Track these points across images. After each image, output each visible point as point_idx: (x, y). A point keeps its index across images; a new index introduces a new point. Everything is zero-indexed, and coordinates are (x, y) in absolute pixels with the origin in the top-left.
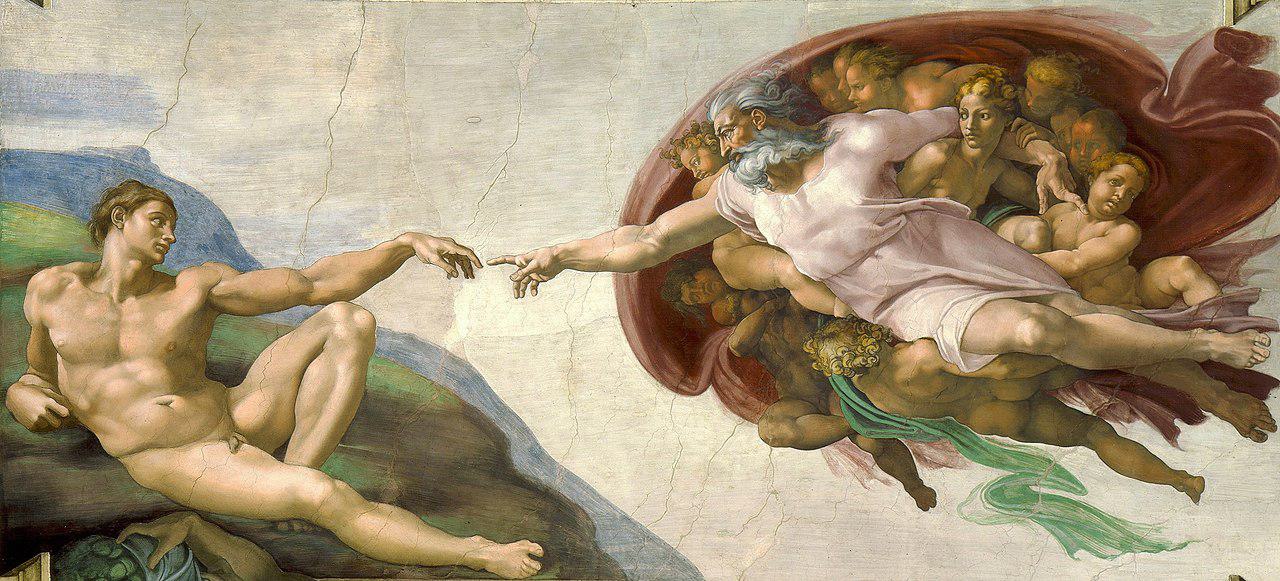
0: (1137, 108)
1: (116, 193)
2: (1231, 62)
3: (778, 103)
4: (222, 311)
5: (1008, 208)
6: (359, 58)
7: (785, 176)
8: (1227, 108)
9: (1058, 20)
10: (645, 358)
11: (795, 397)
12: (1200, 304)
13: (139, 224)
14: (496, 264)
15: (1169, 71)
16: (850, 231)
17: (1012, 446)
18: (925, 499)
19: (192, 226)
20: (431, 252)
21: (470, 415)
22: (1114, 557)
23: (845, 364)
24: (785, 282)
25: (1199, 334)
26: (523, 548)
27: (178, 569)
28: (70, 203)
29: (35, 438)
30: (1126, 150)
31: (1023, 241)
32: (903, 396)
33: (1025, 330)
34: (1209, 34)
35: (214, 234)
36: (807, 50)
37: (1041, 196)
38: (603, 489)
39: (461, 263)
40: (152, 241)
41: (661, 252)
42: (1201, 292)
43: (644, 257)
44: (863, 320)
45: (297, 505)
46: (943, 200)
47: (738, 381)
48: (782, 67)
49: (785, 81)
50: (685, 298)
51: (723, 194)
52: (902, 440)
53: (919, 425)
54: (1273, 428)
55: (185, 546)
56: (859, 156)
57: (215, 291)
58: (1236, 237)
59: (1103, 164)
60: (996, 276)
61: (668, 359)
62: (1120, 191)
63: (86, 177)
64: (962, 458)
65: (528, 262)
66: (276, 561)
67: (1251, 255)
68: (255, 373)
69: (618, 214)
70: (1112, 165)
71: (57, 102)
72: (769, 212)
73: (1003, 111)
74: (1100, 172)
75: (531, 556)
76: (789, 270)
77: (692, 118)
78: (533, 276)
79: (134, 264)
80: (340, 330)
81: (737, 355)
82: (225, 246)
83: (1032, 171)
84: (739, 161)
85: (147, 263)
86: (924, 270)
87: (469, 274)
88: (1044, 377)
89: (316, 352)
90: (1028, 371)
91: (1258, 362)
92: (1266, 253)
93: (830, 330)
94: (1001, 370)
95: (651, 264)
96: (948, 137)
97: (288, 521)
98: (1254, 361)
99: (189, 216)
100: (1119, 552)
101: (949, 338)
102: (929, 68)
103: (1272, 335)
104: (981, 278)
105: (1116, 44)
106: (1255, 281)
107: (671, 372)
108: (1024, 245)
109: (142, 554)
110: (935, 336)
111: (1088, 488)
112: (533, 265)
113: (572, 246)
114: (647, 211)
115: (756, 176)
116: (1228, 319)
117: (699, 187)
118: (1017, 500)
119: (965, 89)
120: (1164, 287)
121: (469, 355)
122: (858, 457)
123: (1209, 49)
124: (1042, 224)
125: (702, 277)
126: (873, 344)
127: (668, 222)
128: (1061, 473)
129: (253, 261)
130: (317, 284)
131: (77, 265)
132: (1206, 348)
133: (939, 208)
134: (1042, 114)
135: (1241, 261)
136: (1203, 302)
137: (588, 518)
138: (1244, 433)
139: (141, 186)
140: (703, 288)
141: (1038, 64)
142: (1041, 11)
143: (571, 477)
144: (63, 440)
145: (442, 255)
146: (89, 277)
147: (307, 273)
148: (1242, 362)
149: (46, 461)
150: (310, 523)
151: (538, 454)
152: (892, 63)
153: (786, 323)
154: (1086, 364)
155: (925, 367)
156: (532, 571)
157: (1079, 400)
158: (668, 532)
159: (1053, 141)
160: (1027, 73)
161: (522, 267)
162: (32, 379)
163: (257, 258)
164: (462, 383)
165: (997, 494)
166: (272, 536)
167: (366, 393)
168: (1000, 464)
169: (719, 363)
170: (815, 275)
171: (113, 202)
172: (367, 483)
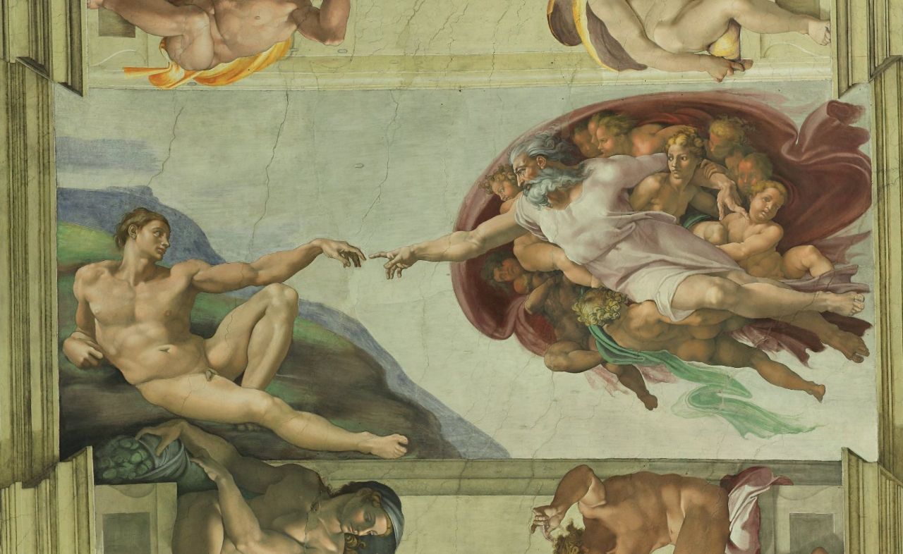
0: (779, 152)
1: (129, 216)
2: (837, 122)
3: (553, 152)
4: (200, 290)
5: (700, 217)
6: (285, 127)
7: (558, 198)
8: (835, 151)
9: (729, 97)
10: (470, 315)
11: (568, 339)
12: (820, 276)
13: (146, 237)
14: (375, 257)
15: (799, 129)
16: (601, 232)
17: (702, 368)
18: (651, 402)
19: (180, 236)
20: (333, 249)
21: (360, 354)
22: (769, 437)
23: (598, 318)
24: (560, 266)
25: (821, 295)
26: (395, 439)
27: (174, 455)
28: (101, 223)
29: (81, 372)
30: (772, 179)
31: (709, 238)
32: (635, 338)
33: (711, 294)
34: (823, 105)
35: (195, 242)
36: (571, 117)
37: (720, 208)
38: (445, 400)
39: (352, 257)
40: (155, 246)
41: (480, 248)
42: (821, 268)
43: (470, 252)
44: (609, 290)
45: (250, 414)
46: (658, 212)
47: (531, 330)
48: (557, 128)
49: (558, 137)
50: (497, 277)
51: (519, 210)
52: (636, 365)
53: (645, 355)
54: (867, 354)
55: (179, 441)
56: (605, 185)
57: (196, 278)
58: (842, 233)
59: (758, 188)
60: (693, 260)
61: (486, 317)
62: (770, 205)
63: (112, 206)
64: (673, 375)
65: (395, 256)
66: (238, 450)
67: (852, 244)
68: (222, 330)
69: (453, 224)
70: (764, 189)
71: (91, 158)
72: (549, 221)
73: (696, 155)
74: (756, 193)
75: (400, 444)
76: (562, 258)
77: (499, 162)
78: (399, 265)
79: (144, 261)
80: (276, 302)
81: (530, 312)
82: (201, 249)
83: (714, 193)
84: (529, 190)
85: (152, 260)
86: (648, 257)
87: (358, 264)
88: (725, 322)
89: (261, 315)
90: (714, 320)
91: (857, 312)
92: (862, 242)
93: (590, 295)
94: (696, 320)
95: (475, 256)
96: (661, 172)
97: (244, 424)
98: (854, 311)
99: (178, 229)
100: (773, 434)
101: (664, 300)
102: (648, 128)
103: (867, 296)
104: (684, 261)
105: (765, 111)
106: (854, 261)
107: (488, 325)
108: (710, 240)
109: (151, 447)
110: (655, 299)
111: (753, 393)
112: (398, 258)
113: (423, 245)
114: (471, 222)
115: (541, 198)
116: (838, 285)
117: (504, 206)
118: (708, 403)
119: (671, 141)
120: (798, 265)
121: (357, 316)
122: (606, 376)
123: (824, 114)
124: (721, 226)
125: (507, 264)
126: (616, 304)
127: (485, 228)
128: (735, 384)
129: (220, 258)
130: (261, 273)
131: (107, 262)
132: (824, 304)
133: (656, 217)
134: (720, 157)
135: (846, 249)
136: (823, 274)
137: (436, 418)
138: (849, 358)
139: (147, 211)
140: (508, 270)
141: (717, 125)
142: (718, 92)
143: (425, 394)
144: (100, 374)
145: (340, 252)
146: (115, 270)
147: (254, 265)
148: (847, 312)
149: (89, 387)
150: (259, 426)
151: (403, 379)
152: (625, 125)
153: (561, 292)
154: (751, 315)
155: (651, 319)
156: (401, 454)
157: (746, 338)
158: (488, 427)
159: (727, 174)
160: (710, 131)
161: (391, 259)
162: (78, 335)
163: (222, 256)
164: (354, 334)
165: (696, 399)
166: (234, 434)
167: (292, 340)
168: (697, 379)
169: (519, 319)
170: (579, 261)
171: (129, 221)
172: (296, 399)
